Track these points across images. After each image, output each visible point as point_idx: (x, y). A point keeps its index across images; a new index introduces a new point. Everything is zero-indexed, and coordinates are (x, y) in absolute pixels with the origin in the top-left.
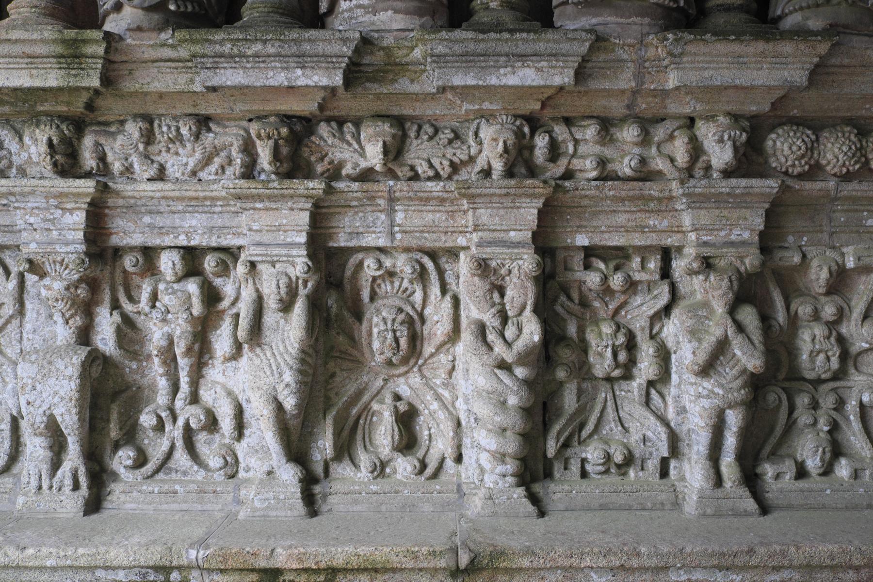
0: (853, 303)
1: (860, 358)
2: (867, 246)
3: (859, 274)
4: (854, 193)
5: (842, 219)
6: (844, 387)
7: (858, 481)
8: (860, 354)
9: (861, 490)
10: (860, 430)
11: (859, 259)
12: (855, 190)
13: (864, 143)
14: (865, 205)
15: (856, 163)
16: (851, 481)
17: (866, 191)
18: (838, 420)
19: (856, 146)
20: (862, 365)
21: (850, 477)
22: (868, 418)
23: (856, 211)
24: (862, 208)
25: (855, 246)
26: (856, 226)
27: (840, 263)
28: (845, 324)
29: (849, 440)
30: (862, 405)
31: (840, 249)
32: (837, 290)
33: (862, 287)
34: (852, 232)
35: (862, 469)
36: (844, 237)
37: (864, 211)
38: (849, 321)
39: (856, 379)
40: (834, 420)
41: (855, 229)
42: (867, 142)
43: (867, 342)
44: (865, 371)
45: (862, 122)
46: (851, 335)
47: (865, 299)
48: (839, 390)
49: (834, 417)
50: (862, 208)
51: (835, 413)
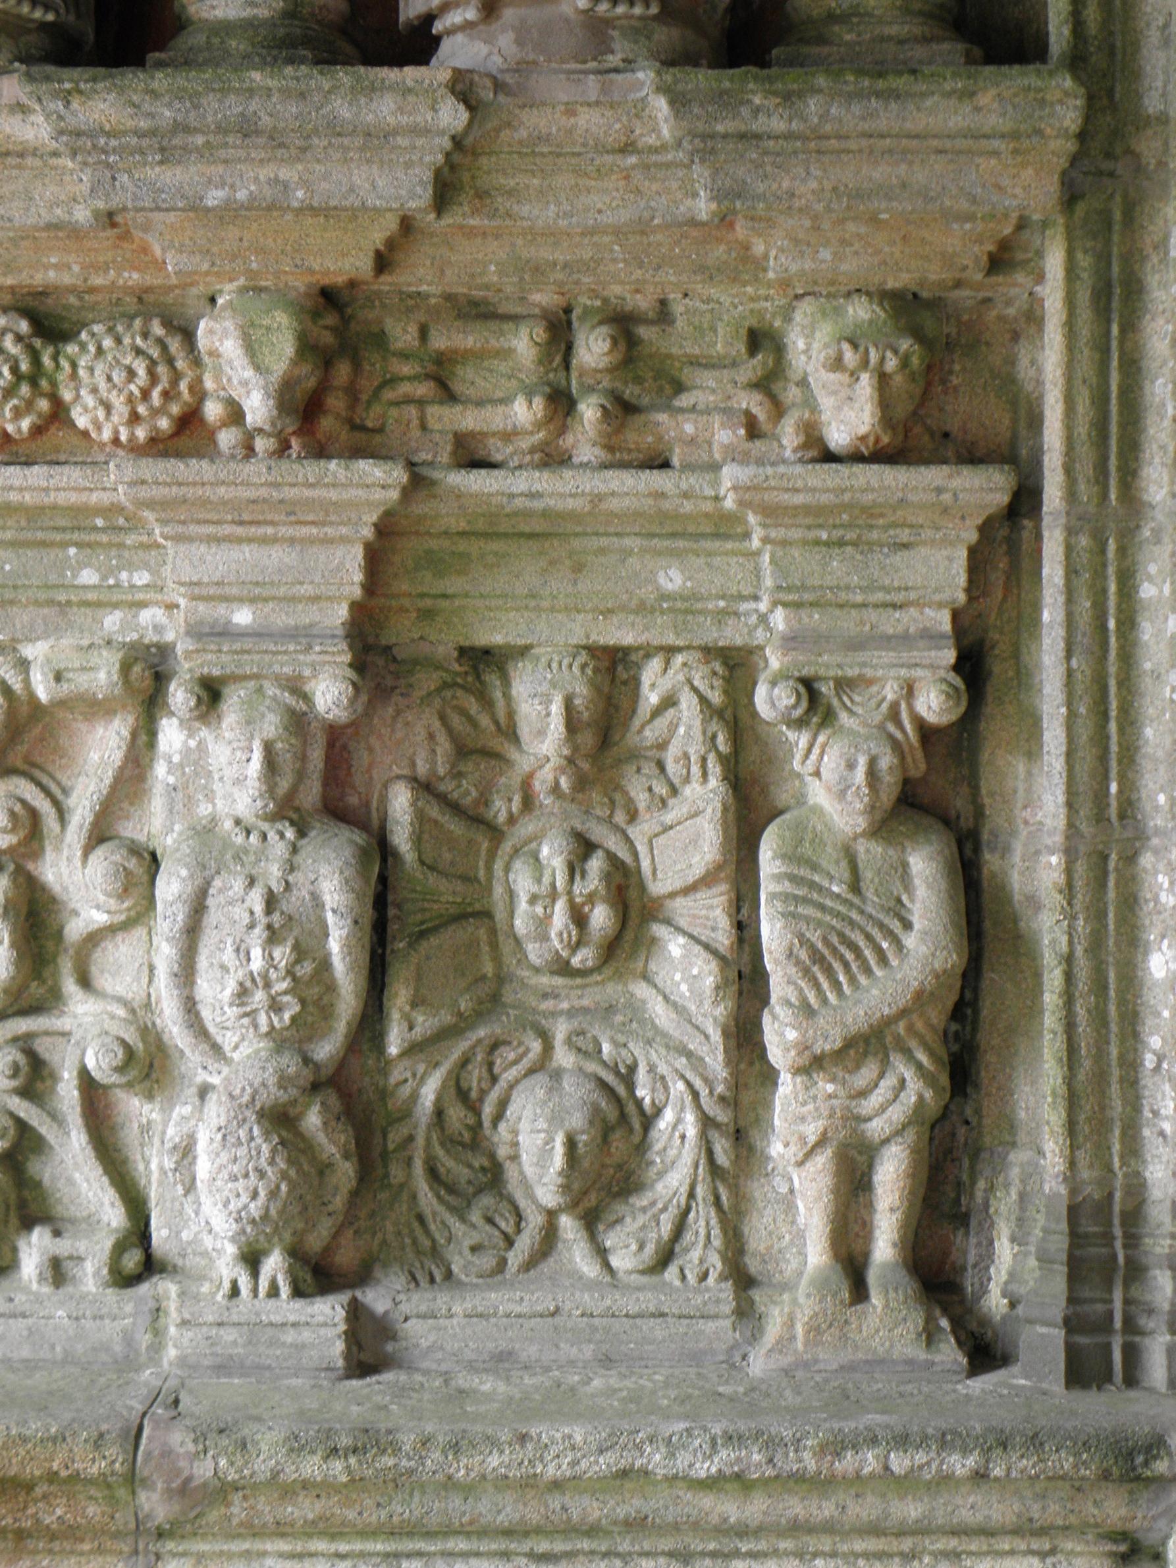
0: (71, 801)
1: (97, 955)
2: (85, 642)
3: (87, 720)
4: (14, 497)
5: (7, 567)
6: (47, 1033)
7: (69, 1289)
8: (94, 938)
9: (60, 1313)
10: (83, 1149)
11: (58, 677)
12: (11, 488)
13: (46, 360)
14: (64, 530)
15: (18, 414)
16: (46, 1289)
17: (46, 490)
18: (34, 1123)
19: (15, 370)
20: (102, 972)
21: (41, 1279)
22: (120, 1120)
23: (43, 544)
24: (58, 537)
25: (51, 641)
26: (48, 587)
27: (17, 687)
28: (49, 855)
29: (71, 1182)
30: (88, 1084)
31: (15, 650)
32: (34, 765)
33: (95, 756)
34: (37, 603)
35: (71, 1258)
36: (22, 617)
37: (65, 545)
38: (57, 849)
39: (80, 1009)
40: (22, 1126)
41: (42, 596)
42: (55, 358)
43: (98, 907)
44: (109, 990)
45: (72, 300)
46: (66, 889)
47: (92, 788)
48: (38, 1041)
49: (22, 1115)
50: (58, 537)
51: (25, 1104)
